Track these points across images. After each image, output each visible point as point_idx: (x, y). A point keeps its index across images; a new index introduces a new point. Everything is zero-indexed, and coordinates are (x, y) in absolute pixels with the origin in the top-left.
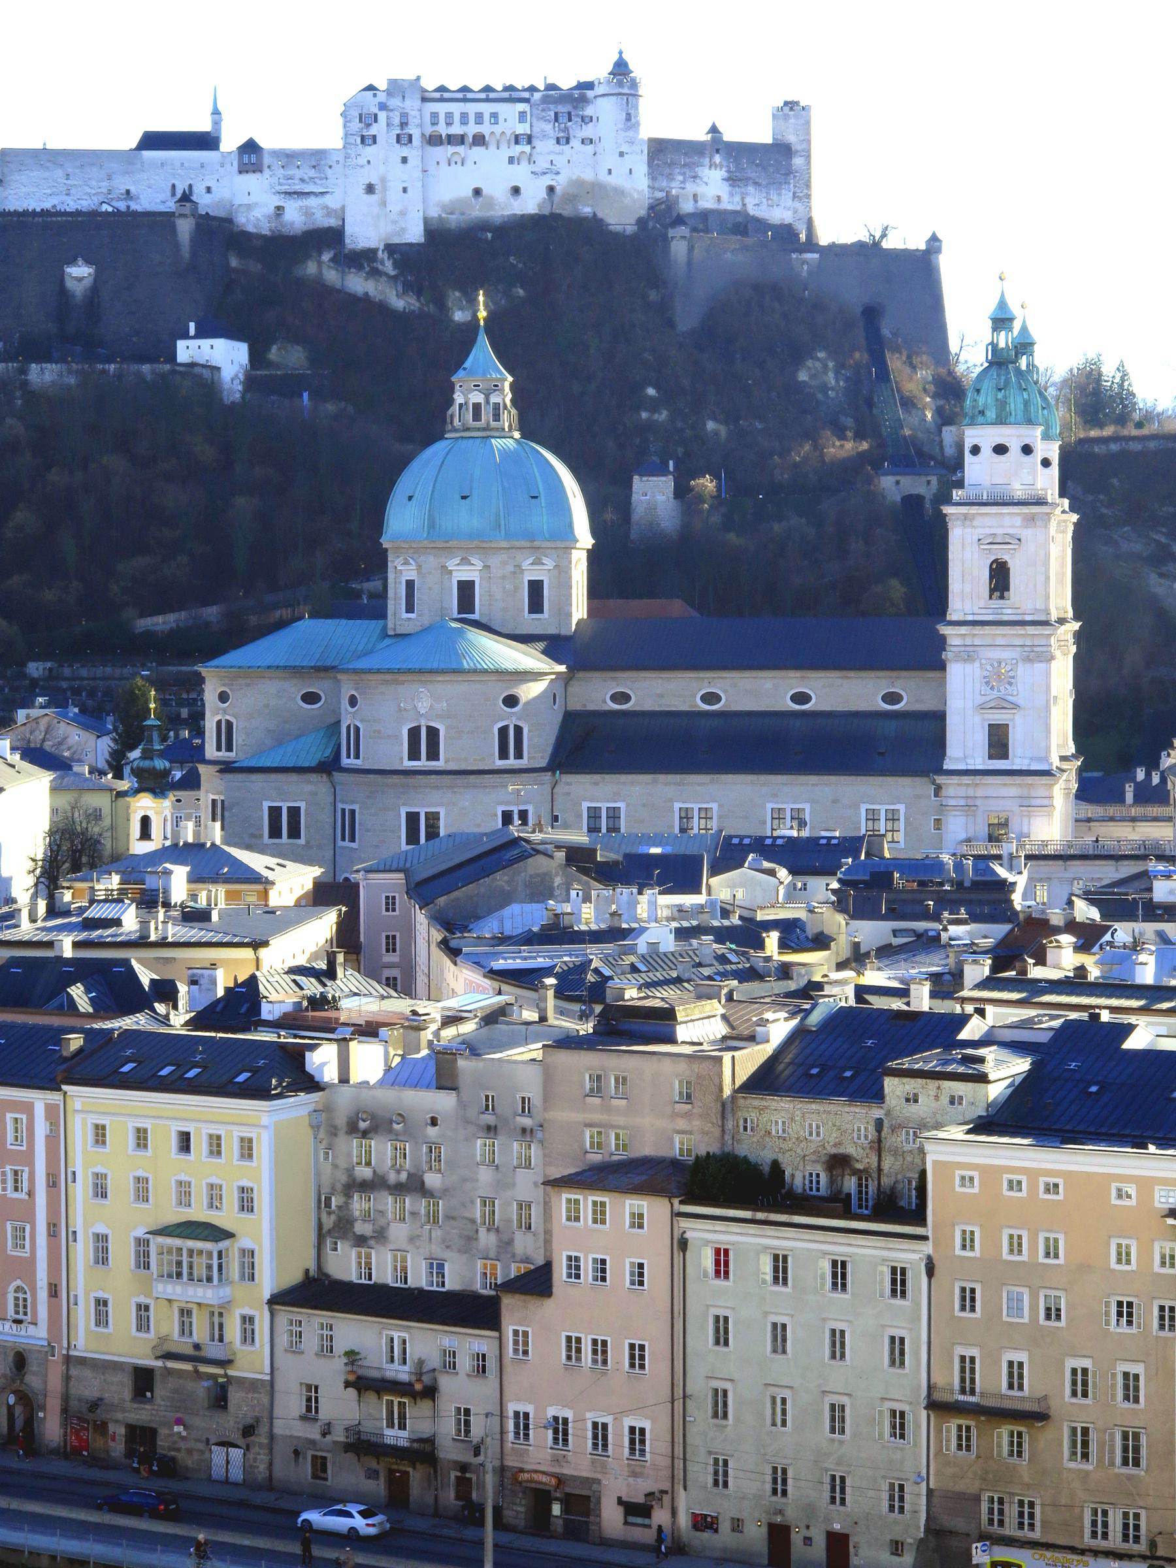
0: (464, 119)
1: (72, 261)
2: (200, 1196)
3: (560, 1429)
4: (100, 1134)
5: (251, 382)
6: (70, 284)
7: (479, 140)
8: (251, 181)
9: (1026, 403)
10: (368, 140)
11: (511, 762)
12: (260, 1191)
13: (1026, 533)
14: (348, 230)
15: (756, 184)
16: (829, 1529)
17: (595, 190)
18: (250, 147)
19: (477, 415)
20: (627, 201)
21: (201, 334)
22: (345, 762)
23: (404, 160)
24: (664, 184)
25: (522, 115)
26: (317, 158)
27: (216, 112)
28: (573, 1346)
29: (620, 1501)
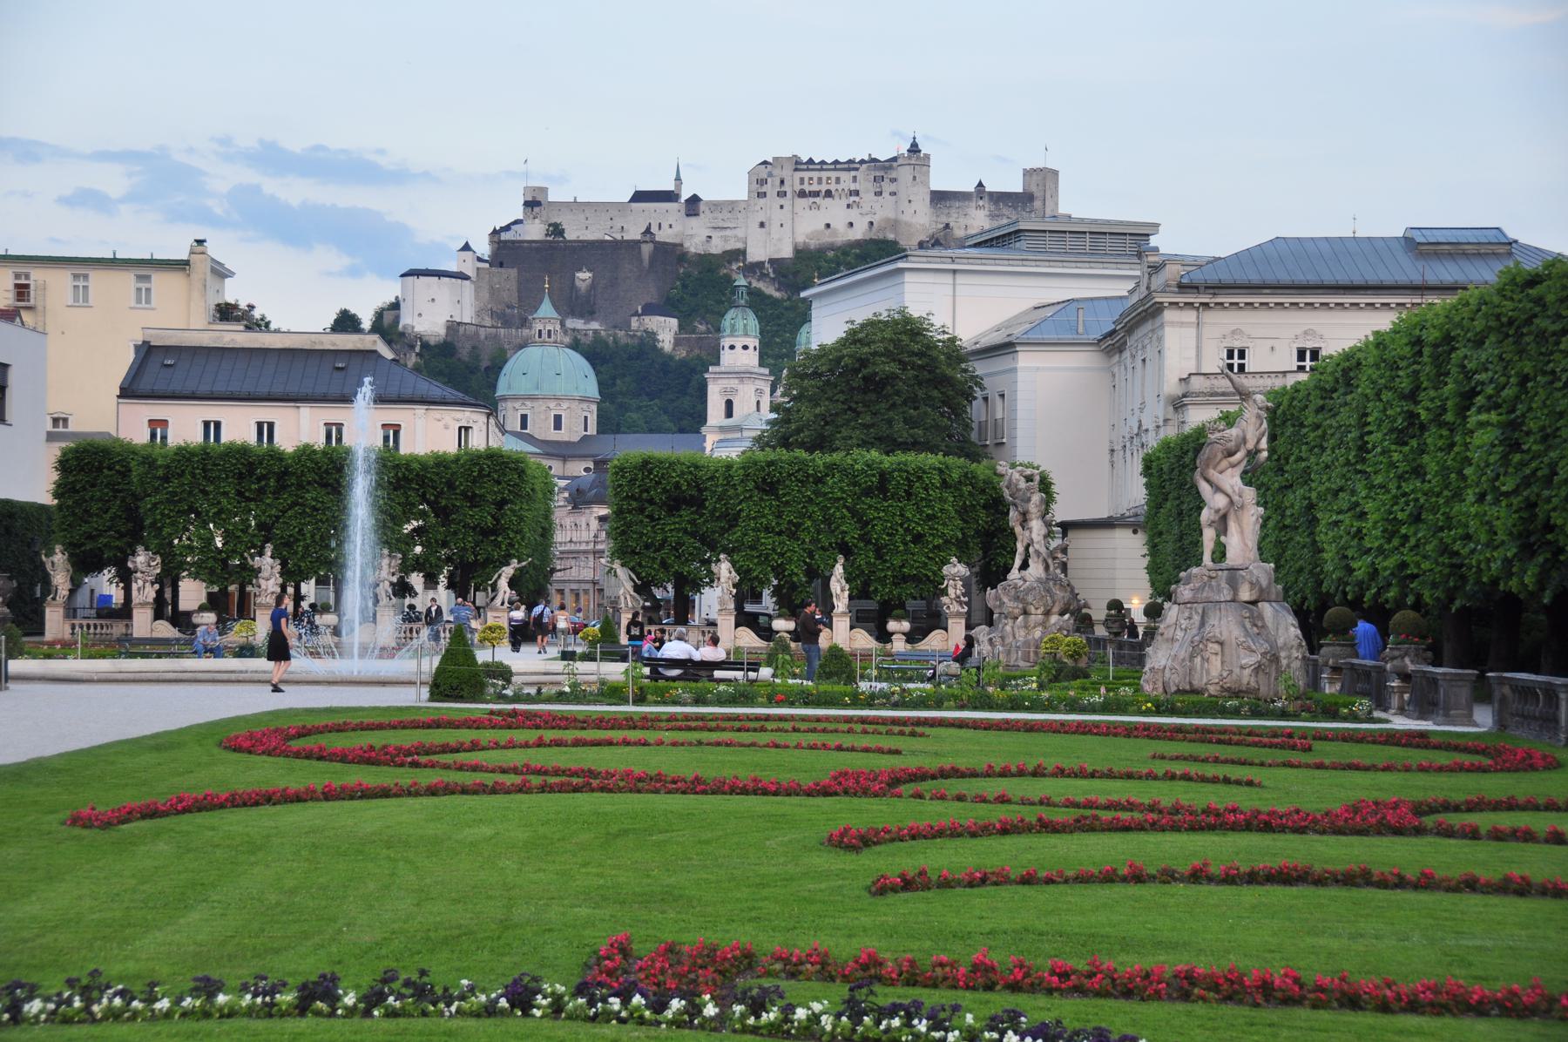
0: (820, 180)
1: (580, 270)
5: (677, 342)
6: (578, 283)
7: (829, 194)
8: (693, 221)
9: (745, 325)
10: (762, 195)
13: (740, 387)
14: (749, 251)
18: (694, 200)
19: (540, 336)
23: (782, 207)
24: (944, 219)
26: (732, 206)
27: (678, 179)
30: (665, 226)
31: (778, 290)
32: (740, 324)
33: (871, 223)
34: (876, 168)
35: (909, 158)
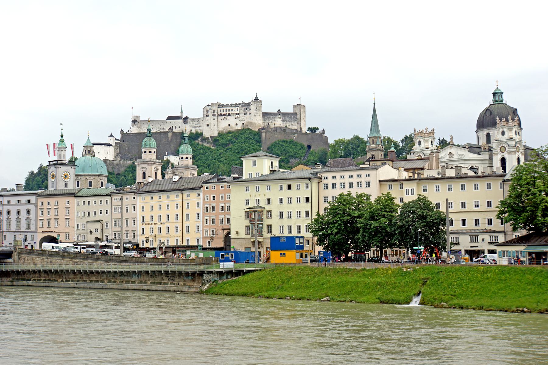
0: (226, 110)
7: (229, 115)
8: (186, 125)
9: (150, 144)
10: (208, 116)
13: (148, 167)
15: (289, 121)
17: (251, 123)
20: (256, 125)
23: (214, 119)
24: (267, 122)
25: (237, 109)
26: (199, 119)
27: (182, 112)
30: (177, 127)
31: (213, 146)
32: (148, 143)
33: (243, 124)
34: (244, 106)
35: (255, 102)
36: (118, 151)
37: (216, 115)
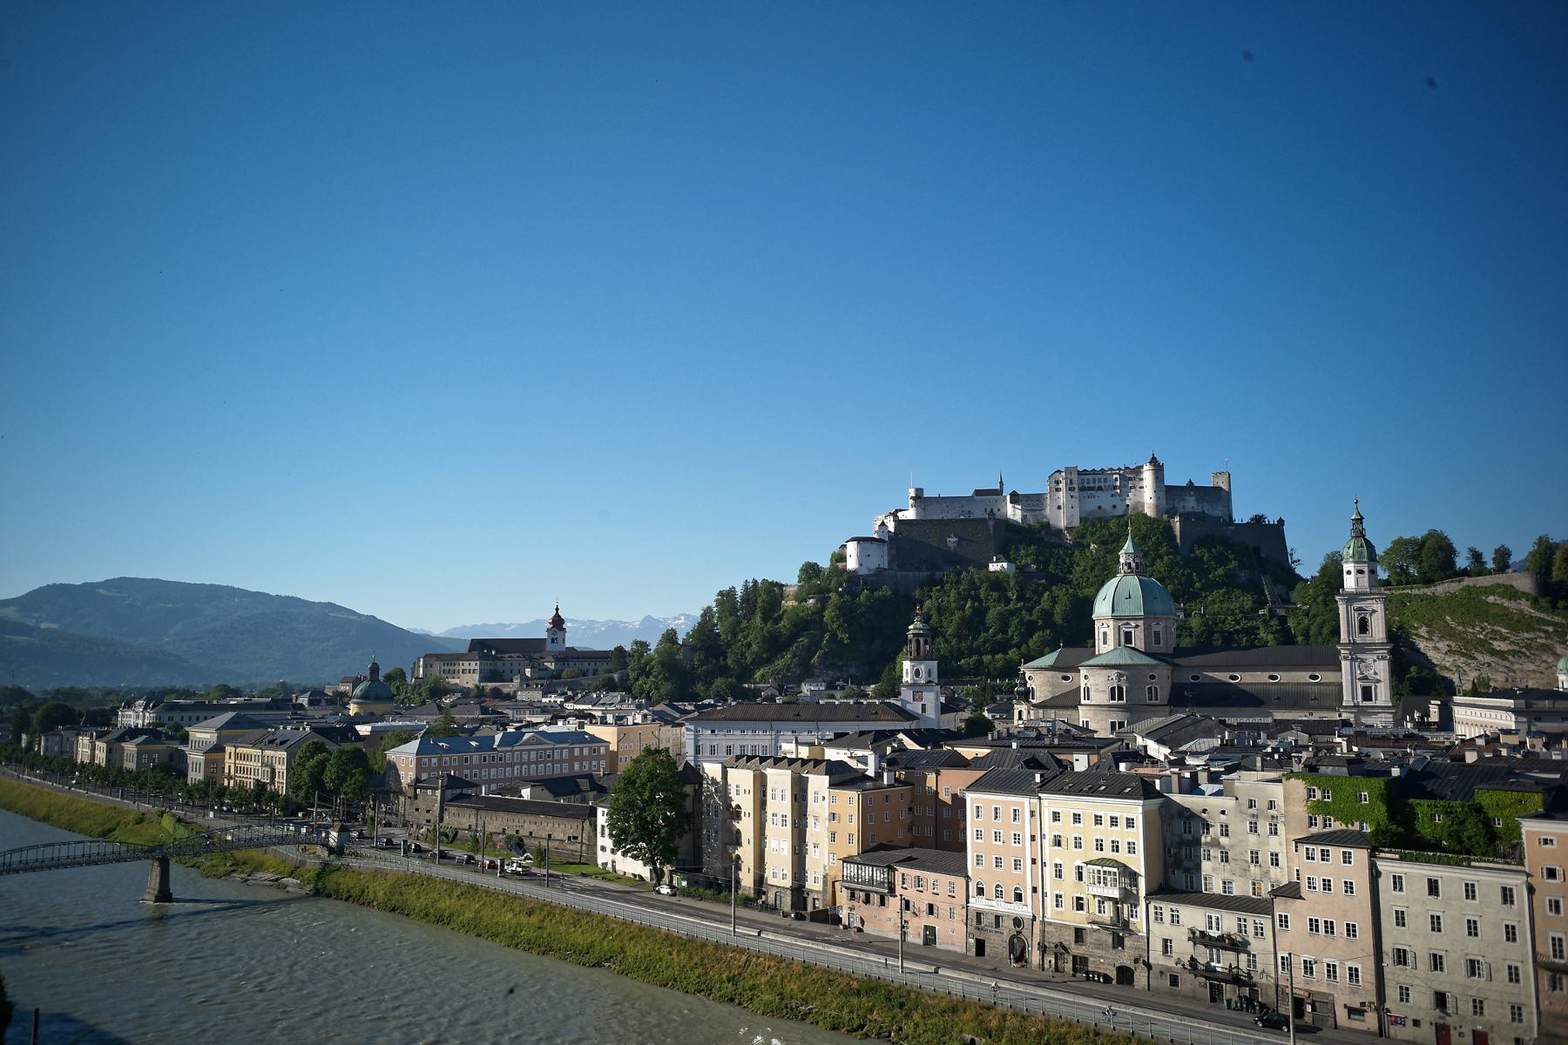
0: (1094, 479)
1: (950, 537)
2: (1107, 846)
3: (1308, 967)
4: (1056, 816)
6: (949, 544)
7: (1100, 489)
10: (1058, 490)
11: (1153, 702)
12: (1138, 845)
15: (1207, 502)
16: (1474, 1028)
21: (998, 561)
22: (1083, 702)
23: (1072, 497)
24: (1171, 502)
27: (1001, 483)
28: (1313, 925)
29: (1345, 1006)
36: (895, 553)
37: (1077, 490)
